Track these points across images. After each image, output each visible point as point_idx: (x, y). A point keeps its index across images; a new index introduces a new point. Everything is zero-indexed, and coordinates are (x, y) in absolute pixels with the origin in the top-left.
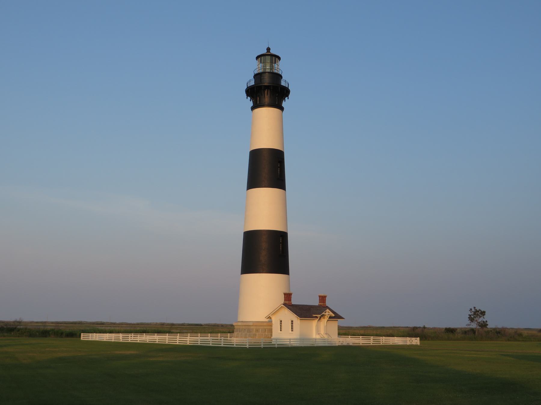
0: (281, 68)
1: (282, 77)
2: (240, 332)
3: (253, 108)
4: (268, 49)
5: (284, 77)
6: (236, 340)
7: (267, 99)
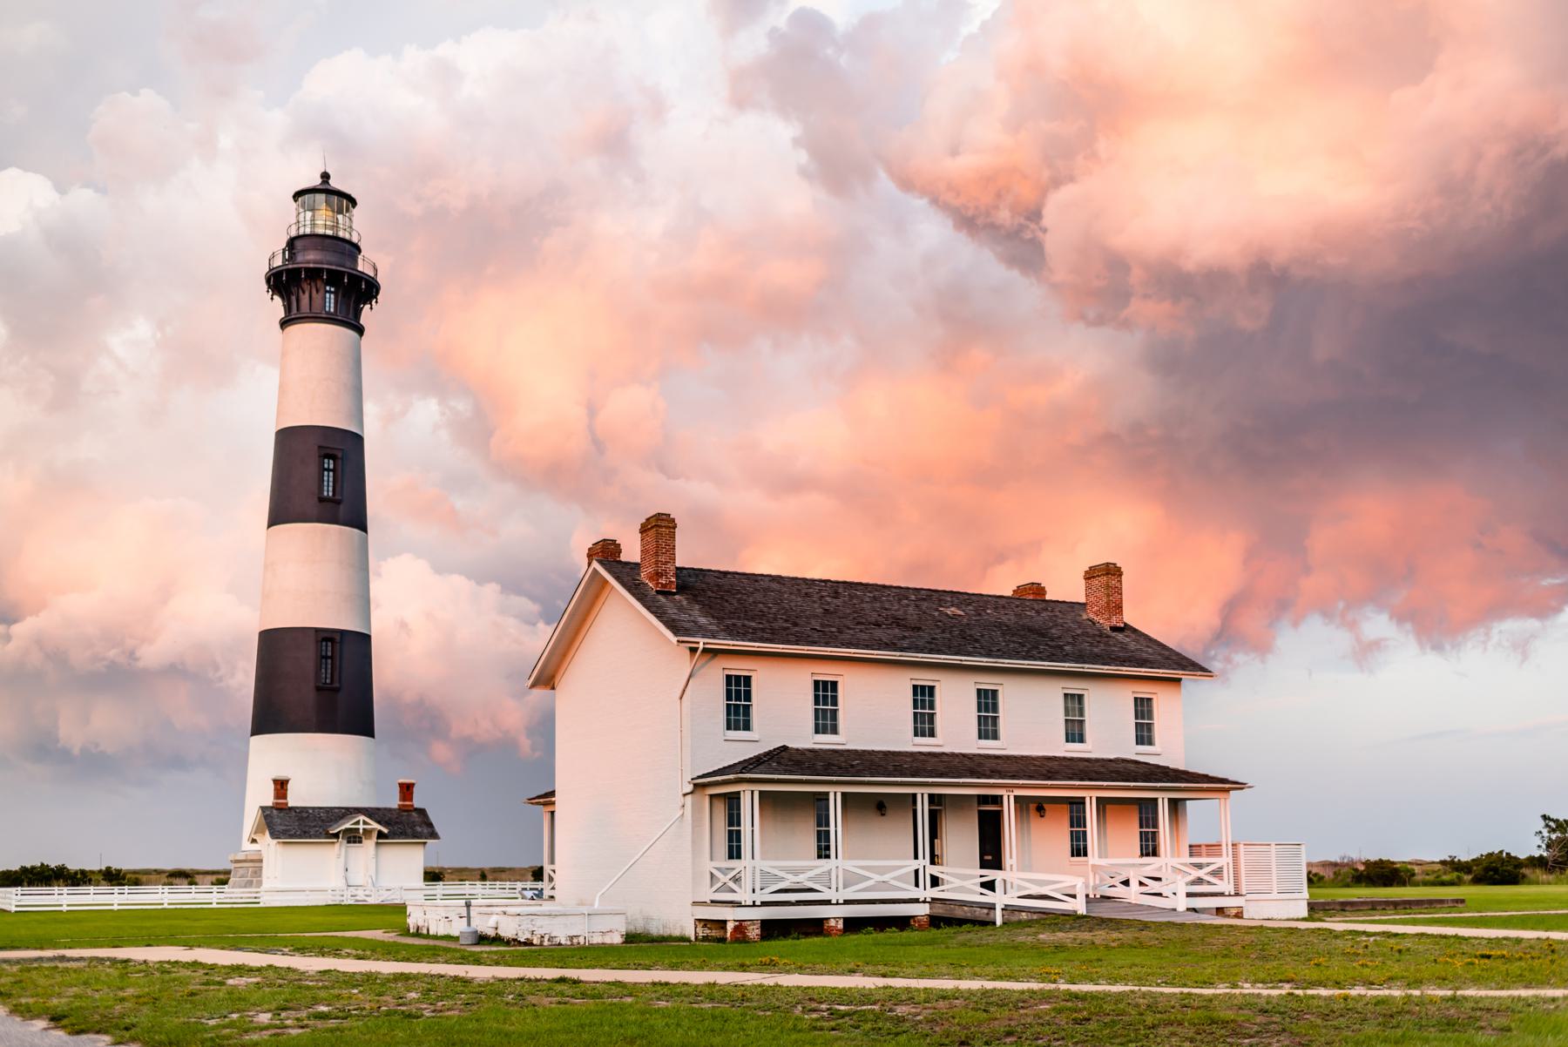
0: (360, 226)
1: (359, 250)
3: (284, 324)
4: (325, 177)
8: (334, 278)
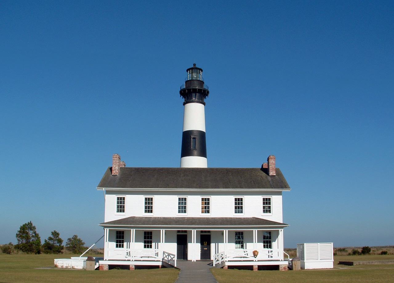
1: (203, 83)
3: (184, 104)
4: (194, 65)
5: (205, 83)
8: (200, 91)
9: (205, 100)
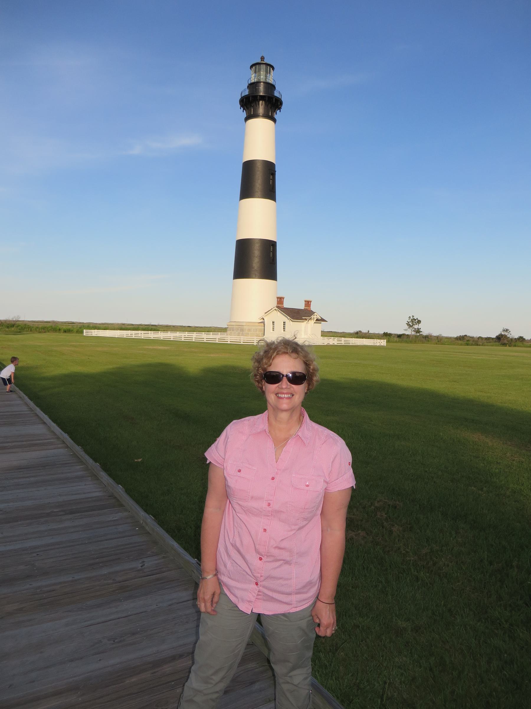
2: (233, 331)
3: (247, 119)
4: (262, 58)
6: (229, 338)
7: (261, 109)
9: (276, 116)
